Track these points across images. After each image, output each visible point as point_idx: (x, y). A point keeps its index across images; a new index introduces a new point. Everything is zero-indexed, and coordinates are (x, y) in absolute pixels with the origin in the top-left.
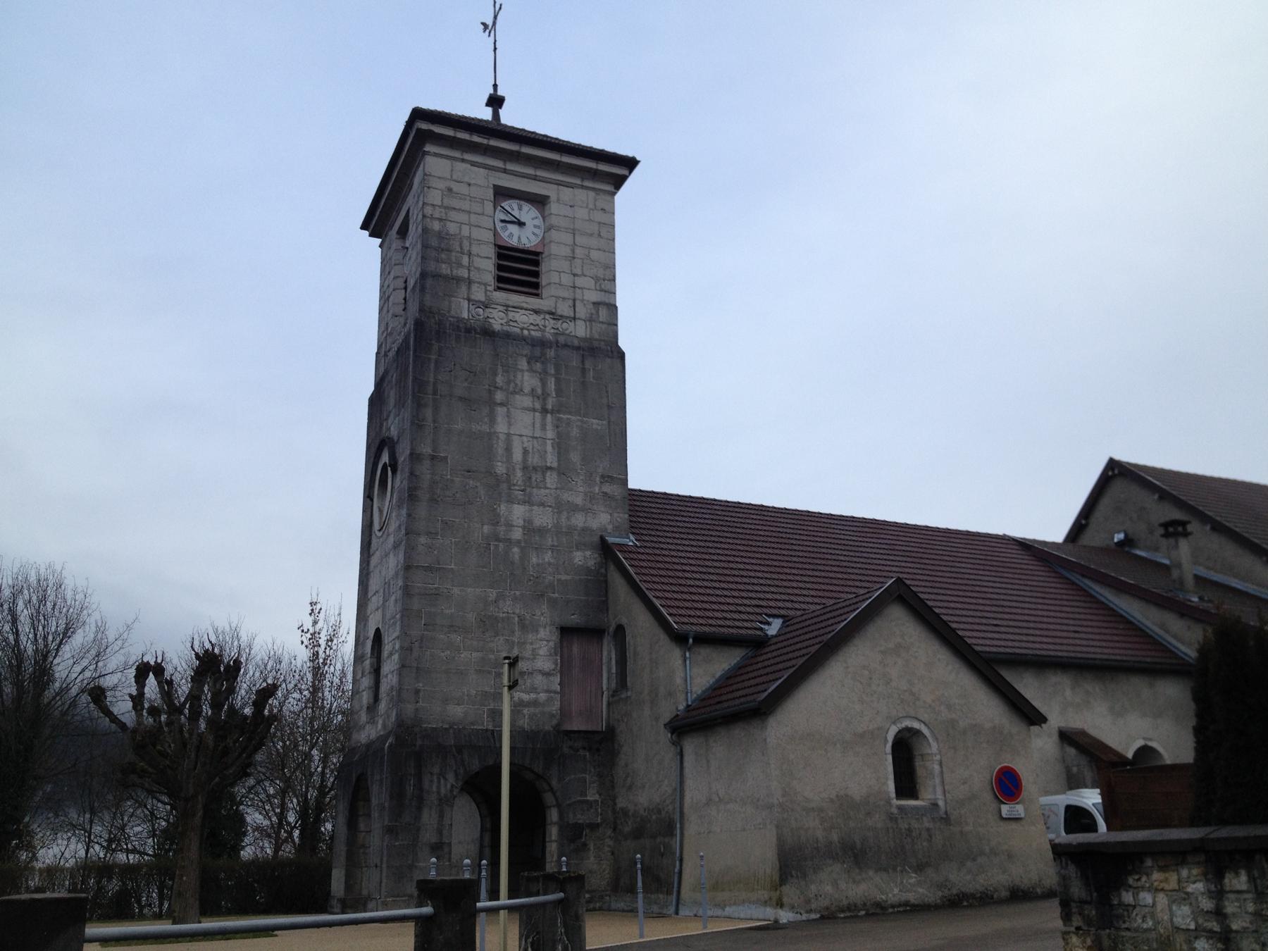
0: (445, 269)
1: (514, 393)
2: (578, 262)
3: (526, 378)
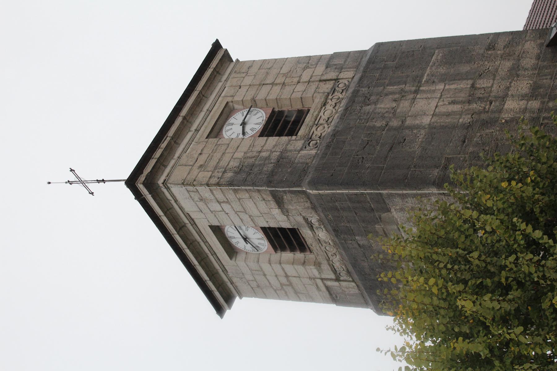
0: (270, 167)
1: (394, 113)
2: (288, 80)
3: (382, 106)
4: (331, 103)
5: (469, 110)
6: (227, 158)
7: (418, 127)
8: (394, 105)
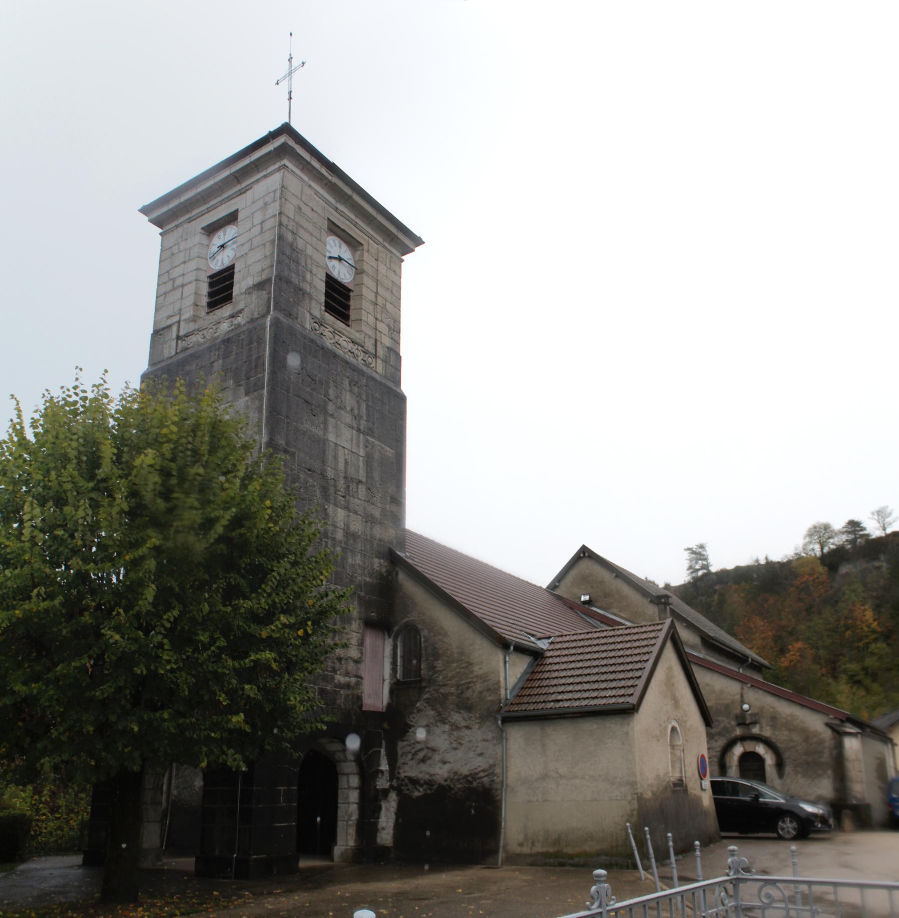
0: (294, 279)
1: (340, 408)
3: (348, 397)
4: (354, 348)
6: (306, 236)
8: (348, 409)
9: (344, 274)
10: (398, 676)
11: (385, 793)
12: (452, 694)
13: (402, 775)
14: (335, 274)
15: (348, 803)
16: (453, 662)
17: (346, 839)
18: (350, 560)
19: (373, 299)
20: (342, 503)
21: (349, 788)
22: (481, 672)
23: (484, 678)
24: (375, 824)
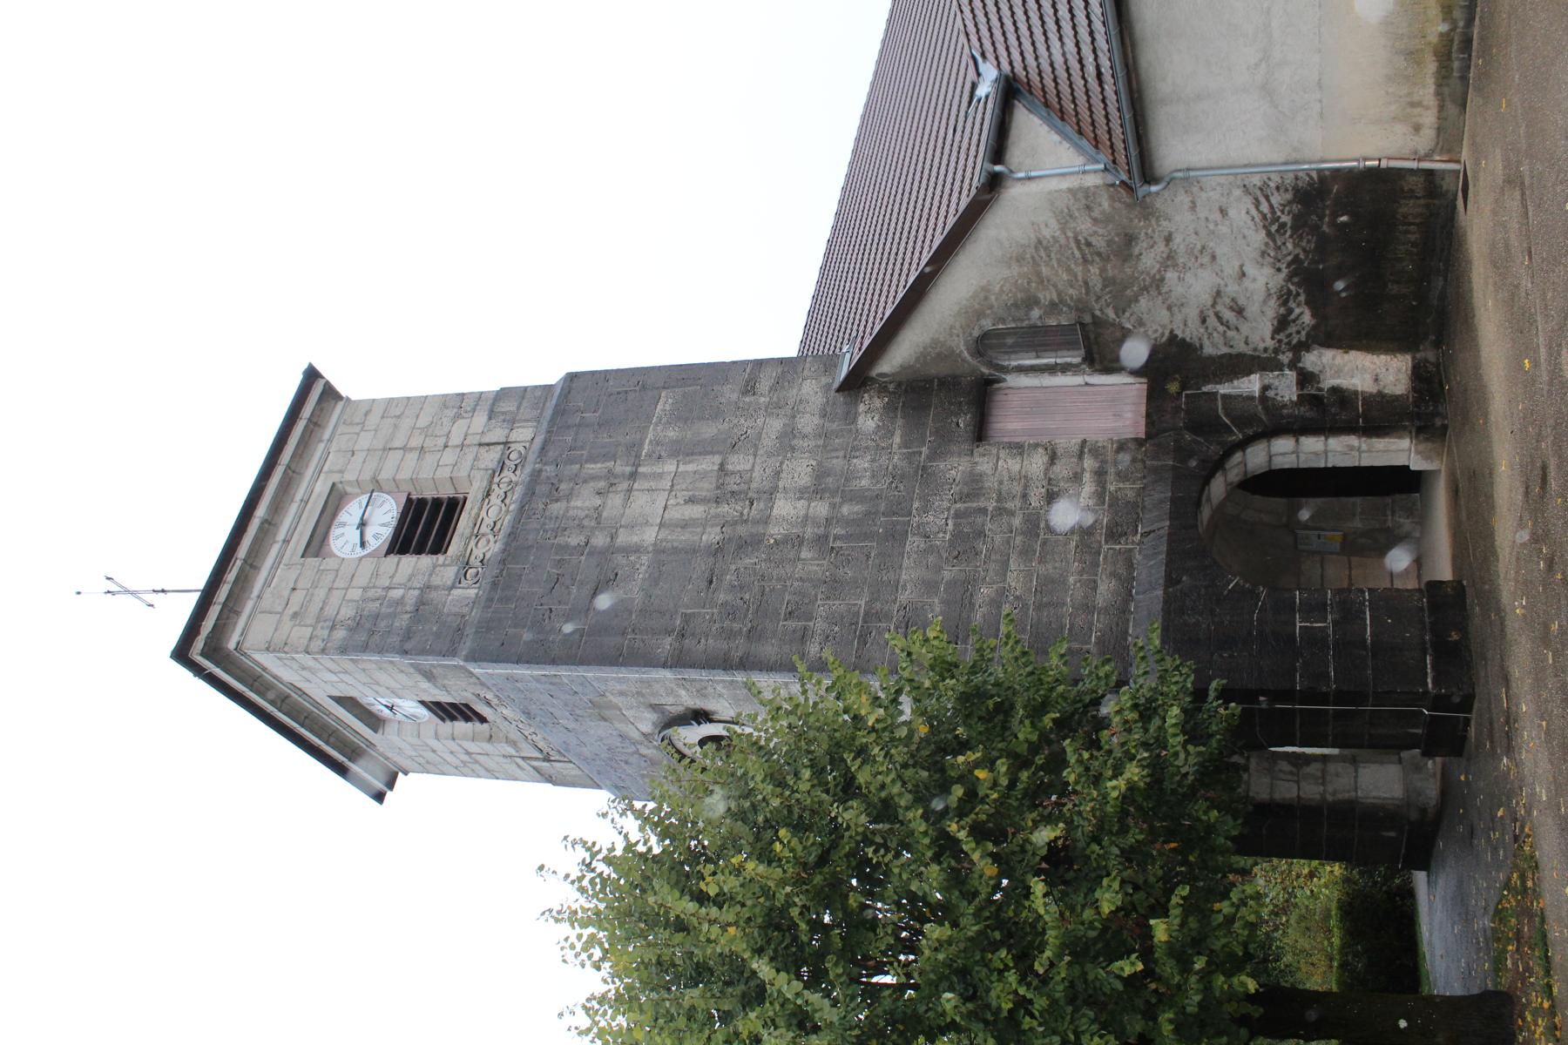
0: (403, 621)
1: (598, 519)
2: (429, 443)
3: (579, 503)
4: (498, 492)
5: (717, 516)
6: (336, 597)
7: (638, 549)
9: (385, 516)
10: (1077, 360)
11: (1305, 378)
12: (1103, 270)
13: (1270, 343)
14: (387, 533)
15: (1326, 452)
16: (1039, 274)
17: (1397, 451)
18: (865, 483)
19: (415, 455)
20: (762, 505)
21: (1296, 452)
22: (1054, 224)
23: (1065, 218)
24: (1369, 399)
